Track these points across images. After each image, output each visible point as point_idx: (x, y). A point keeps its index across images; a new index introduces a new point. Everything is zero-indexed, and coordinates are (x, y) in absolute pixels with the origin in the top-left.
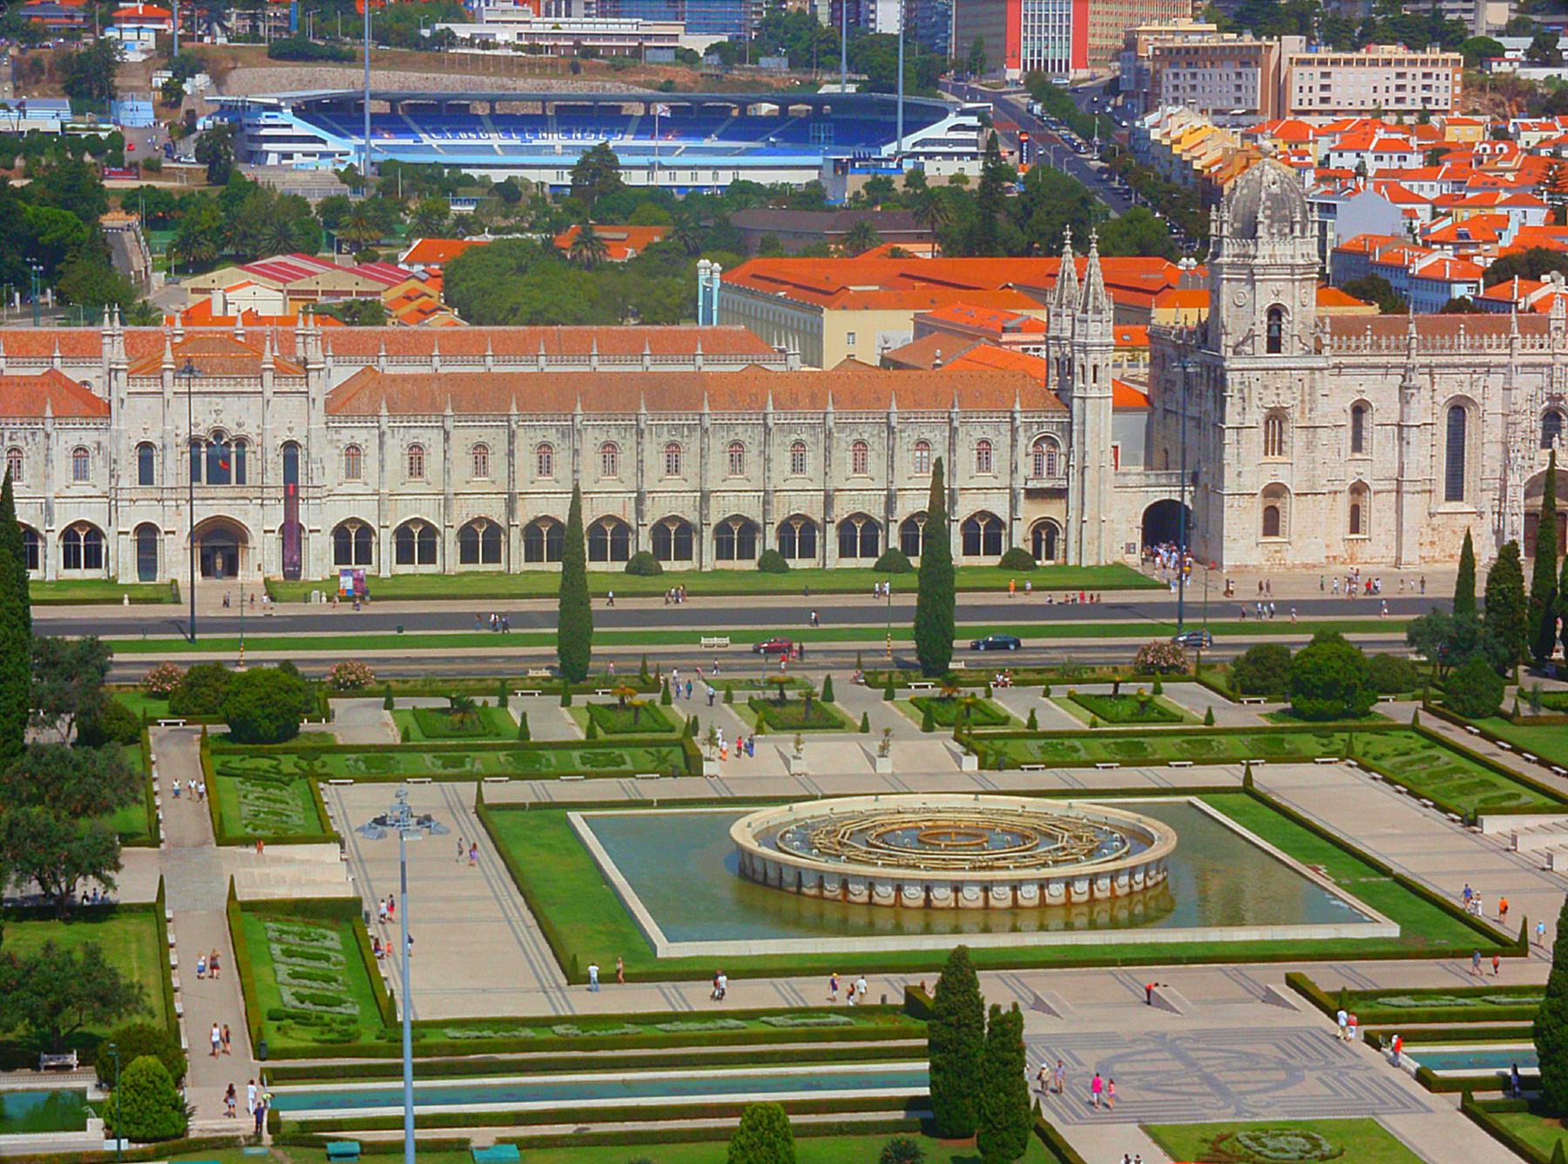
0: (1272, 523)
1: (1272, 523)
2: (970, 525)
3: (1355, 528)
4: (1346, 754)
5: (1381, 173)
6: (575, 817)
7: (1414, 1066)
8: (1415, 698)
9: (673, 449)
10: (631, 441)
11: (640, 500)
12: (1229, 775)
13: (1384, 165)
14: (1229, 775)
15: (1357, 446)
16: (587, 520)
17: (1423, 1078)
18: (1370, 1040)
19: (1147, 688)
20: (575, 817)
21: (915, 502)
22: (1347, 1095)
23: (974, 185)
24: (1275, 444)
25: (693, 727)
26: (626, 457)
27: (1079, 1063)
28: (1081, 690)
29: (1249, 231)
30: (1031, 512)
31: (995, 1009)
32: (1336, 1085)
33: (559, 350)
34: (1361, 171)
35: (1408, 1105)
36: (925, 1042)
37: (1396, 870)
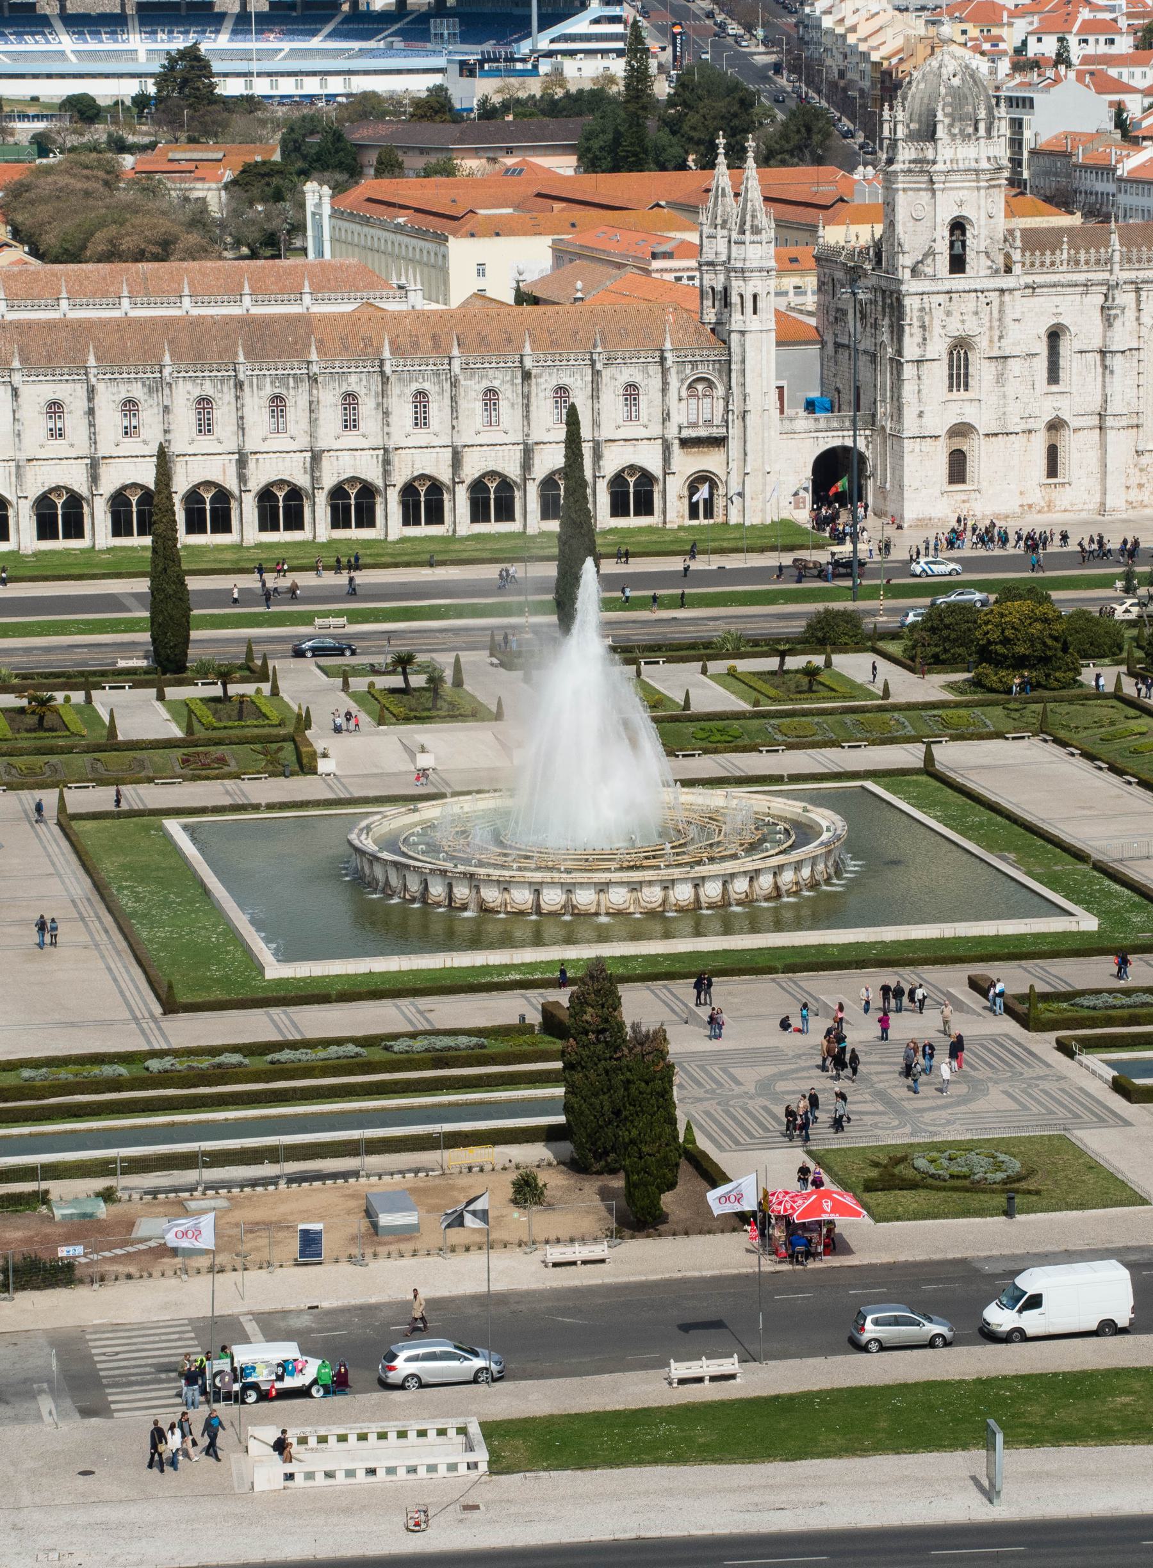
0: (958, 468)
1: (958, 468)
2: (618, 482)
3: (1052, 471)
4: (1044, 730)
5: (1086, 60)
6: (173, 826)
7: (1110, 1073)
8: (1118, 663)
9: (277, 404)
10: (229, 394)
11: (242, 463)
12: (908, 756)
13: (1090, 50)
14: (908, 756)
15: (1054, 376)
16: (181, 485)
17: (1120, 1087)
18: (1064, 1047)
19: (818, 660)
20: (173, 826)
21: (551, 459)
22: (1035, 1108)
23: (618, 89)
24: (959, 378)
25: (304, 721)
26: (223, 415)
27: (738, 1083)
28: (744, 666)
29: (927, 133)
30: (686, 464)
31: (636, 1027)
32: (1025, 1099)
33: (144, 292)
34: (1062, 59)
35: (1104, 1118)
36: (559, 1065)
37: (1096, 856)
